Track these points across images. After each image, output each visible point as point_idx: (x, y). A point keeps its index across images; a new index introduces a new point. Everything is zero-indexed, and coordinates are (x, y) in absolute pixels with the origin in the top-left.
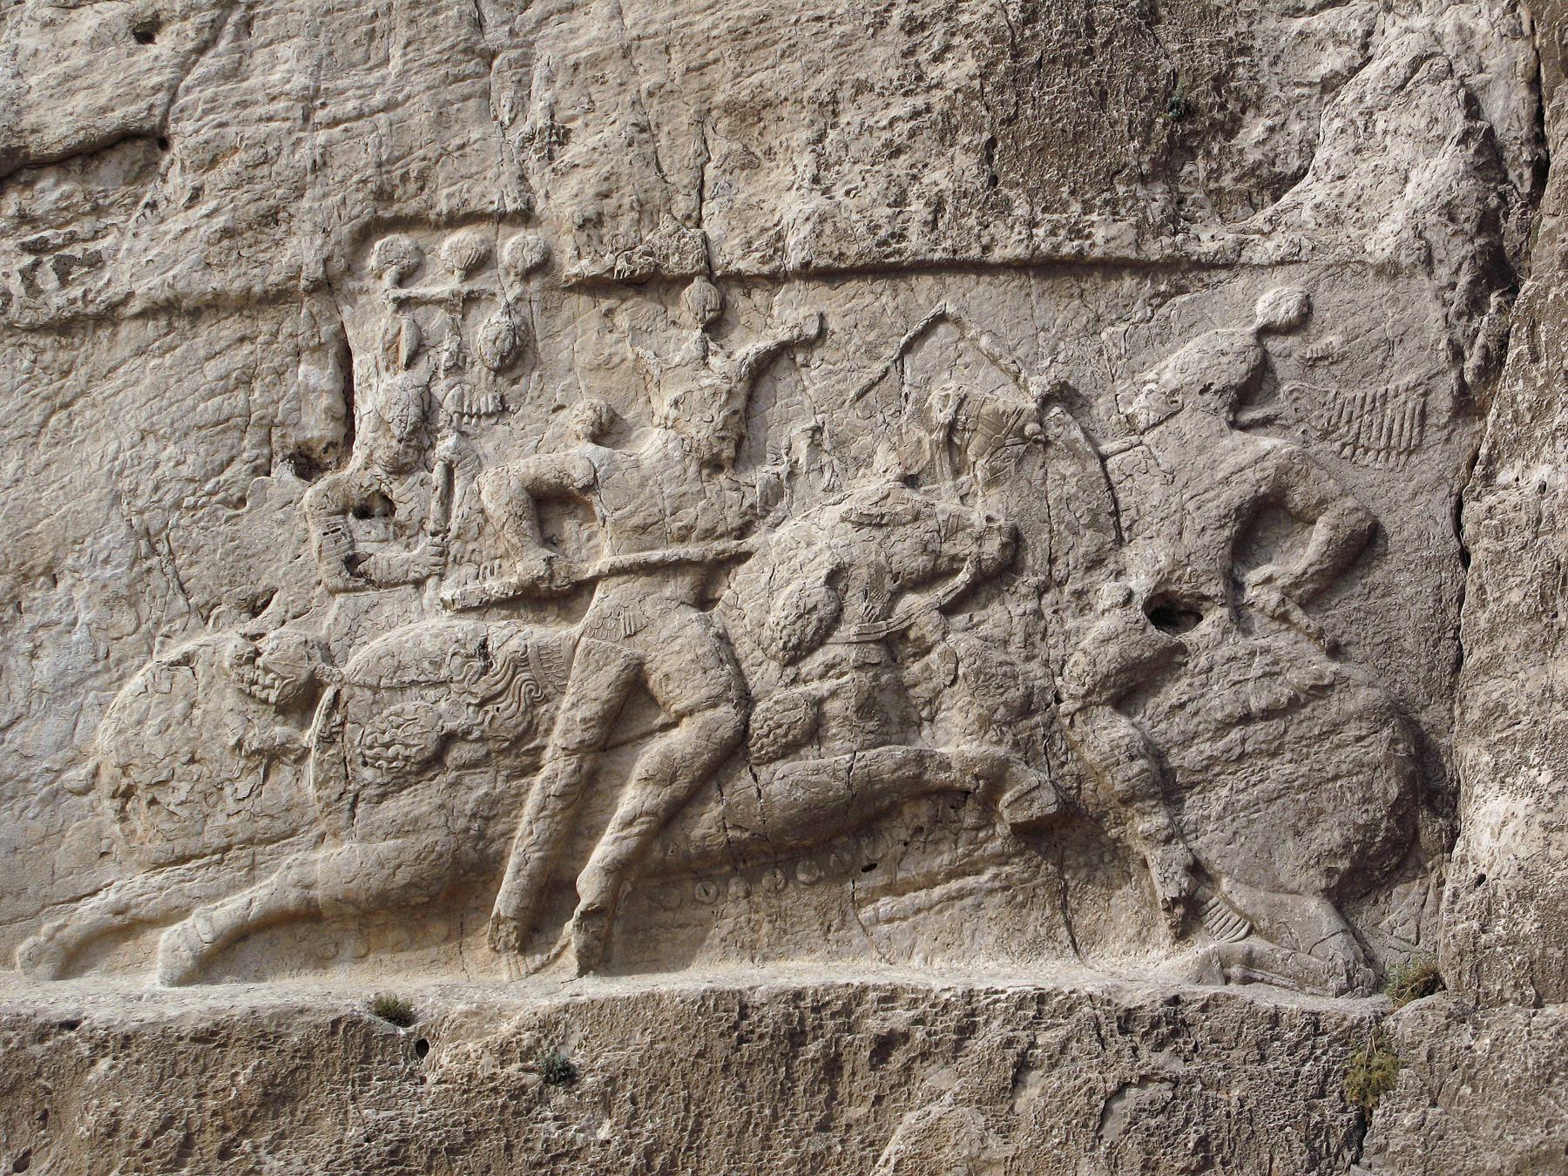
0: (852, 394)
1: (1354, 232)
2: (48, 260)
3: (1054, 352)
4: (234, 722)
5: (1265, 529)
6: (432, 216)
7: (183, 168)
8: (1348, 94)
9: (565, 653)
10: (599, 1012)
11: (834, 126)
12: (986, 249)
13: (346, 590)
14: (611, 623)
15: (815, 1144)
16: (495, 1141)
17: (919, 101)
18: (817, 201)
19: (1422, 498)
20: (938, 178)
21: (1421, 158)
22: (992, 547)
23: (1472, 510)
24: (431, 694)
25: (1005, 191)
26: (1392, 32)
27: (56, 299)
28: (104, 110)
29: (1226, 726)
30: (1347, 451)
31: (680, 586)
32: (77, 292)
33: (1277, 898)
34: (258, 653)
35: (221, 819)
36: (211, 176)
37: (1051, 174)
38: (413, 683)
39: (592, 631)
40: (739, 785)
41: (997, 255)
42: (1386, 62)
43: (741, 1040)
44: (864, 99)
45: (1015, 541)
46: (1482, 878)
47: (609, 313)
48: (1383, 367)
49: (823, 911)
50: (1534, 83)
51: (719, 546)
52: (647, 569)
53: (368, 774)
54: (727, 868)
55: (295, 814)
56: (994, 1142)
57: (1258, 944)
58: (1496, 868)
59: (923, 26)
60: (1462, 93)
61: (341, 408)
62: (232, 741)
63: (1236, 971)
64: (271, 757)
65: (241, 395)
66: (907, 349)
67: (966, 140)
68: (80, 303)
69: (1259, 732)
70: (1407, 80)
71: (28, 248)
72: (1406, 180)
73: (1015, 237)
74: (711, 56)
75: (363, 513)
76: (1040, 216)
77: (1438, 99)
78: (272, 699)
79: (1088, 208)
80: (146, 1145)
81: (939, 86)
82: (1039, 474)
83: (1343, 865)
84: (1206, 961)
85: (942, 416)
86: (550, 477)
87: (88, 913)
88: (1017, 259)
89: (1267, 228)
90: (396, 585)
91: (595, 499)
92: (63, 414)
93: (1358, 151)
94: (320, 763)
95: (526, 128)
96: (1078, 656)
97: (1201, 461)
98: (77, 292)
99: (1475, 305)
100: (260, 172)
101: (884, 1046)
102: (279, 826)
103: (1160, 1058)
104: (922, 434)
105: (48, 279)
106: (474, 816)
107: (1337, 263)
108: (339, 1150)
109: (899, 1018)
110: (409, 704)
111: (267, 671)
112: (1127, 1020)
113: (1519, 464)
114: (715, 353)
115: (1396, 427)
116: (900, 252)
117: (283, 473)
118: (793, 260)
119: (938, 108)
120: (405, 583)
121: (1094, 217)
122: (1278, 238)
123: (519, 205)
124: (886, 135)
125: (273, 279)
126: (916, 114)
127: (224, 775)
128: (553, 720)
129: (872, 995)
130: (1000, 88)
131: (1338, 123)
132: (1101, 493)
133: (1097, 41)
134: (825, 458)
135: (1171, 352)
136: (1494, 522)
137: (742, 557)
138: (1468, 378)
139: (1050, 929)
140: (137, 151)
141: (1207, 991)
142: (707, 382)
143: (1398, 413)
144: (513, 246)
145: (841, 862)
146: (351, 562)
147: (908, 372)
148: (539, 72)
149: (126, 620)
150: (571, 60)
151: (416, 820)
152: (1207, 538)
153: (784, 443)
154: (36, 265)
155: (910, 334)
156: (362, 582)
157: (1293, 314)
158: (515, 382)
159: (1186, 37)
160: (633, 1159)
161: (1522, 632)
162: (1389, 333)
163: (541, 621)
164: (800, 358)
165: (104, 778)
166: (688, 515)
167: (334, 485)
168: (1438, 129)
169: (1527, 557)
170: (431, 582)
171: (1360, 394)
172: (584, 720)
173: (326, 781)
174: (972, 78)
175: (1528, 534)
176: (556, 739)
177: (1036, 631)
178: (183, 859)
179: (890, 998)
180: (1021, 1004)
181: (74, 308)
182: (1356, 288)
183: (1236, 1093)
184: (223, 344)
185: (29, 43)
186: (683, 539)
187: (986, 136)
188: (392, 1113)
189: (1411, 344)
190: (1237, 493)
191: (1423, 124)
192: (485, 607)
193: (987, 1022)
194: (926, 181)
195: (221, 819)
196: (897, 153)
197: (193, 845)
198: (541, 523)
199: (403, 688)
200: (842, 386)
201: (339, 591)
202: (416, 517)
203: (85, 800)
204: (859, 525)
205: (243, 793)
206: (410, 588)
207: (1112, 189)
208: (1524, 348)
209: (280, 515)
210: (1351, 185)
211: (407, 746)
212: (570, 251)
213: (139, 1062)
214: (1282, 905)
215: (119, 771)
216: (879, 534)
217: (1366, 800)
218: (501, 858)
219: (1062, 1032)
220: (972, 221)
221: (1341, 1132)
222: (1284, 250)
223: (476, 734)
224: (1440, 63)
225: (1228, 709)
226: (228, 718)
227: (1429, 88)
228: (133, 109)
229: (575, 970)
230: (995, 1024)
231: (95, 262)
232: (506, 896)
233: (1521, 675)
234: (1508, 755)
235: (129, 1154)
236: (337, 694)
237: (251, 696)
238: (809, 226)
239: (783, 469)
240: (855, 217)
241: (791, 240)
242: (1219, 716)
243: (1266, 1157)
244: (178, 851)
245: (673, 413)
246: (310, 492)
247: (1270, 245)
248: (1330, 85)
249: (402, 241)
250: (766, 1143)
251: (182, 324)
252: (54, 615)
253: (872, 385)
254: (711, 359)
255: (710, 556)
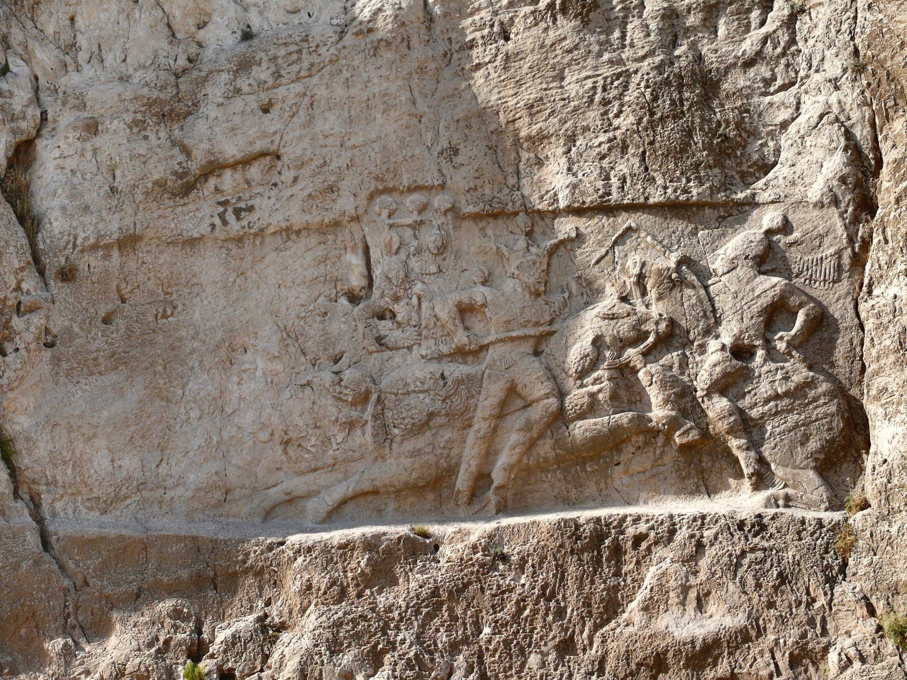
0: (593, 262)
1: (803, 189)
2: (230, 210)
3: (679, 242)
4: (335, 411)
5: (777, 316)
6: (401, 188)
7: (289, 168)
8: (792, 129)
9: (479, 376)
10: (513, 531)
11: (574, 146)
12: (647, 198)
13: (377, 351)
14: (498, 363)
15: (612, 582)
16: (475, 586)
17: (611, 135)
18: (571, 179)
19: (841, 301)
20: (622, 168)
21: (827, 157)
22: (663, 326)
23: (862, 307)
24: (421, 396)
25: (652, 173)
26: (808, 102)
27: (235, 226)
28: (251, 143)
29: (767, 401)
30: (807, 282)
31: (528, 347)
32: (245, 223)
33: (796, 471)
34: (341, 380)
35: (331, 452)
36: (302, 171)
37: (672, 166)
38: (414, 391)
39: (490, 366)
40: (560, 431)
41: (651, 201)
42: (808, 116)
43: (577, 539)
44: (586, 134)
45: (672, 323)
46: (885, 461)
47: (483, 229)
48: (820, 246)
49: (597, 483)
50: (873, 125)
51: (541, 329)
52: (513, 339)
53: (396, 431)
54: (555, 466)
55: (364, 448)
56: (691, 578)
57: (790, 491)
58: (892, 456)
59: (609, 102)
60: (843, 129)
61: (365, 271)
62: (333, 418)
63: (781, 502)
64: (351, 425)
65: (322, 266)
66: (615, 243)
67: (633, 151)
68: (247, 228)
69: (784, 403)
70: (818, 124)
71: (220, 203)
72: (822, 166)
73: (658, 193)
74: (517, 116)
75: (381, 317)
76: (668, 184)
77: (831, 133)
78: (350, 400)
79: (688, 180)
80: (325, 593)
81: (618, 128)
82: (679, 295)
83: (822, 456)
84: (768, 499)
85: (636, 271)
86: (466, 301)
87: (275, 494)
88: (660, 203)
89: (764, 187)
90: (399, 349)
91: (486, 310)
92: (243, 278)
93: (799, 154)
94: (374, 427)
95: (439, 148)
96: (702, 372)
97: (748, 287)
98: (245, 223)
99: (856, 220)
100: (323, 170)
101: (638, 540)
102: (357, 454)
103: (757, 540)
104: (625, 278)
105: (230, 217)
106: (444, 448)
107: (796, 202)
108: (408, 592)
109: (643, 527)
110: (412, 400)
111: (346, 388)
112: (741, 525)
113: (883, 287)
114: (532, 246)
115: (827, 271)
116: (609, 201)
117: (343, 301)
118: (562, 204)
119: (619, 138)
120: (403, 348)
121: (691, 184)
122: (769, 191)
123: (440, 182)
124: (598, 150)
125: (331, 217)
126: (610, 140)
127: (331, 433)
128: (476, 406)
129: (629, 519)
130: (646, 129)
131: (789, 142)
132: (707, 305)
133: (685, 108)
134: (584, 290)
135: (728, 241)
136: (876, 311)
137: (551, 334)
138: (857, 250)
139: (697, 487)
140: (267, 161)
141: (772, 511)
142: (529, 258)
143: (829, 265)
144: (440, 201)
145: (606, 462)
146: (379, 340)
147: (617, 252)
148: (442, 124)
149: (278, 366)
150: (456, 118)
151: (419, 450)
152: (753, 321)
153: (565, 283)
154: (226, 211)
155: (616, 235)
156: (384, 348)
157: (780, 224)
158: (444, 259)
159: (722, 105)
160: (536, 591)
161: (892, 358)
162: (821, 232)
163: (465, 363)
164: (569, 247)
165: (276, 436)
166: (528, 315)
167: (368, 306)
168: (834, 145)
169: (891, 326)
170: (415, 347)
171: (811, 258)
172: (491, 405)
173: (377, 434)
174: (633, 124)
175: (891, 316)
176: (479, 414)
177: (684, 363)
178: (315, 470)
179: (637, 520)
180: (695, 520)
181: (244, 230)
182: (805, 212)
183: (790, 553)
184: (312, 245)
185: (213, 115)
186: (525, 326)
187: (641, 149)
188: (429, 576)
189: (831, 237)
190: (765, 301)
191: (827, 142)
192: (440, 358)
193: (680, 528)
194: (617, 169)
195: (331, 452)
196: (603, 157)
197: (319, 464)
198: (463, 321)
199: (408, 393)
200: (588, 259)
201: (374, 352)
202: (406, 319)
203: (268, 445)
204: (604, 319)
205: (340, 440)
206: (405, 350)
207: (698, 172)
208: (881, 237)
209: (343, 319)
210: (798, 168)
211: (413, 419)
212: (464, 202)
213: (316, 558)
214: (798, 474)
215: (283, 433)
216: (613, 322)
217: (830, 429)
218: (458, 464)
219: (714, 531)
220: (639, 187)
221: (836, 568)
222: (772, 197)
223: (443, 412)
224: (832, 117)
225: (769, 393)
226: (330, 408)
227: (829, 127)
228: (264, 142)
229: (494, 512)
230: (684, 528)
231: (251, 209)
232: (463, 481)
233: (893, 376)
234: (891, 409)
235: (317, 597)
236: (379, 397)
237: (341, 399)
238: (568, 190)
239: (566, 295)
240: (588, 185)
241: (560, 196)
242: (765, 396)
243: (807, 579)
244: (313, 466)
245: (516, 272)
246: (356, 309)
247: (766, 194)
248: (784, 125)
249: (387, 199)
250: (592, 582)
251: (293, 237)
252: (247, 366)
253: (602, 258)
254: (530, 248)
255: (538, 334)
